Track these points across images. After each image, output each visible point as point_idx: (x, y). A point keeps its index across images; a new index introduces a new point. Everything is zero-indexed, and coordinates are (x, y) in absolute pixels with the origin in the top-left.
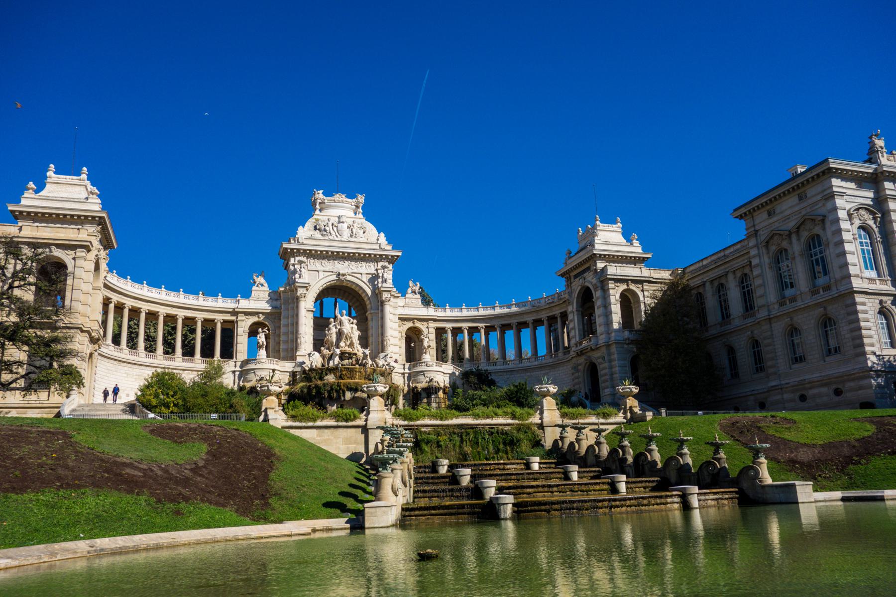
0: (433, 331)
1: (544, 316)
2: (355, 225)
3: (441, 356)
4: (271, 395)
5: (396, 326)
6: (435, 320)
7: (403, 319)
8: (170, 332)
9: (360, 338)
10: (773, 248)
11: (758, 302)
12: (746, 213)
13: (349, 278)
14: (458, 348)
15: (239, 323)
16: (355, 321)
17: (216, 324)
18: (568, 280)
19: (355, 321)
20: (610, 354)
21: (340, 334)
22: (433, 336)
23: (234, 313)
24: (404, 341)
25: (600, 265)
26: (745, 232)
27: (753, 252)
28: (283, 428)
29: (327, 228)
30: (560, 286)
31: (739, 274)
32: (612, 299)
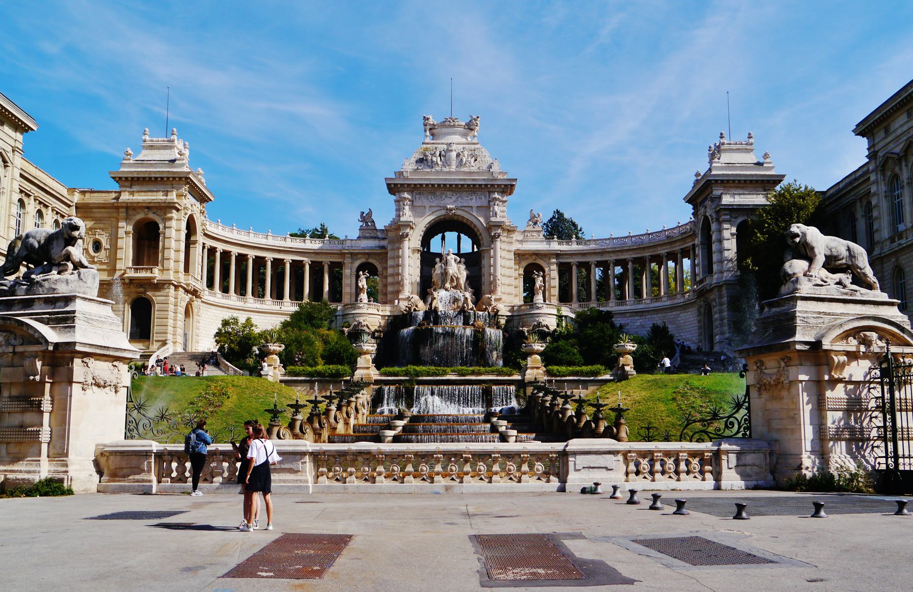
0: (554, 267)
1: (677, 248)
2: (466, 153)
3: (565, 297)
4: (272, 354)
5: (512, 263)
6: (558, 255)
7: (520, 256)
8: (259, 281)
9: (468, 277)
10: (889, 173)
11: (877, 237)
12: (865, 129)
13: (459, 212)
14: (585, 284)
16: (463, 260)
17: (323, 267)
18: (695, 208)
19: (463, 260)
20: (721, 297)
21: (445, 274)
22: (555, 274)
23: (342, 254)
24: (522, 280)
25: (717, 192)
26: (867, 153)
27: (873, 177)
28: (281, 381)
29: (434, 159)
30: (684, 215)
31: (864, 203)
32: (726, 234)
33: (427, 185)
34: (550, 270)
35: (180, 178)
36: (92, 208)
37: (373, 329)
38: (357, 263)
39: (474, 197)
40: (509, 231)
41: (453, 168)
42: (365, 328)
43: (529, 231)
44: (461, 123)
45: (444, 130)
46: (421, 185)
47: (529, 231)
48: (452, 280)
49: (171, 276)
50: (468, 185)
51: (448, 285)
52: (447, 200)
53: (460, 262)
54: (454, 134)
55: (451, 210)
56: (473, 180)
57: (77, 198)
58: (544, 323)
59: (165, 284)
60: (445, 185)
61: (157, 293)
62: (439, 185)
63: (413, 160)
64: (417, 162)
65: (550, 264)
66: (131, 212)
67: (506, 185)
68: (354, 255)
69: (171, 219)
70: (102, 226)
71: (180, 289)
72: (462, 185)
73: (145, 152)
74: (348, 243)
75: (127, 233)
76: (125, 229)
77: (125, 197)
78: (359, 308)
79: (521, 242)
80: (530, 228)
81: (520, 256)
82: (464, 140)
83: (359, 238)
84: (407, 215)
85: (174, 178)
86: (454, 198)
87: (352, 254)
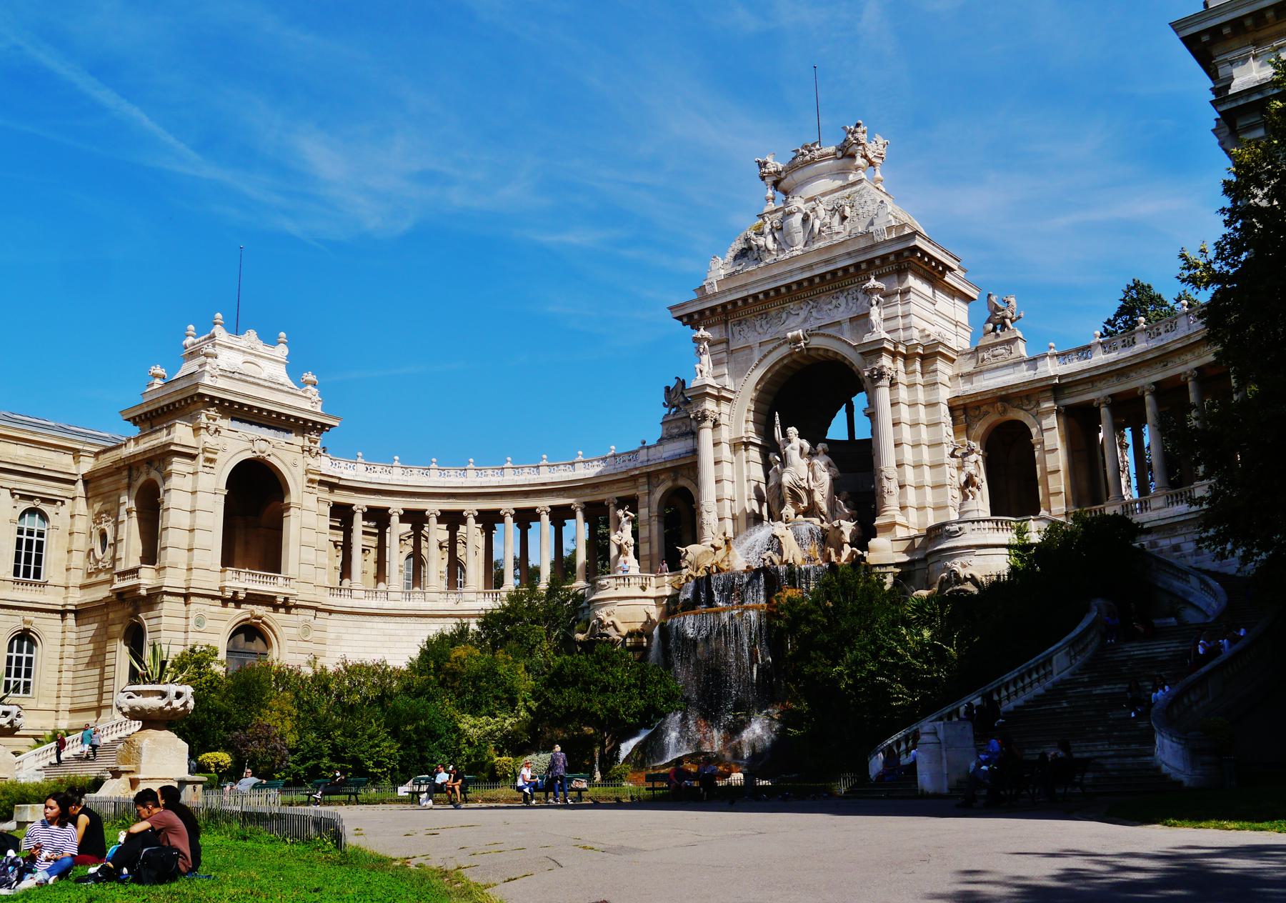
0: (1052, 421)
6: (1057, 388)
7: (963, 411)
9: (837, 487)
13: (816, 342)
15: (643, 500)
23: (634, 479)
33: (745, 299)
34: (1042, 431)
35: (192, 397)
36: (100, 478)
37: (624, 630)
38: (659, 493)
39: (842, 300)
40: (923, 358)
41: (799, 249)
42: (611, 631)
43: (987, 348)
44: (824, 150)
45: (799, 176)
46: (734, 303)
47: (987, 348)
48: (796, 498)
49: (174, 580)
50: (822, 276)
51: (789, 510)
52: (792, 321)
53: (812, 454)
54: (818, 176)
55: (796, 340)
56: (827, 262)
57: (87, 465)
58: (963, 573)
59: (157, 595)
60: (777, 290)
61: (151, 614)
62: (766, 293)
63: (730, 255)
64: (736, 258)
65: (1039, 416)
66: (134, 473)
67: (898, 254)
68: (651, 477)
69: (170, 475)
70: (108, 506)
71: (193, 599)
72: (811, 280)
73: (185, 366)
74: (643, 456)
75: (129, 512)
76: (128, 502)
77: (132, 449)
78: (602, 587)
79: (968, 376)
80: (991, 339)
81: (963, 411)
82: (839, 183)
83: (661, 441)
84: (705, 373)
85: (185, 399)
86: (803, 314)
87: (648, 475)
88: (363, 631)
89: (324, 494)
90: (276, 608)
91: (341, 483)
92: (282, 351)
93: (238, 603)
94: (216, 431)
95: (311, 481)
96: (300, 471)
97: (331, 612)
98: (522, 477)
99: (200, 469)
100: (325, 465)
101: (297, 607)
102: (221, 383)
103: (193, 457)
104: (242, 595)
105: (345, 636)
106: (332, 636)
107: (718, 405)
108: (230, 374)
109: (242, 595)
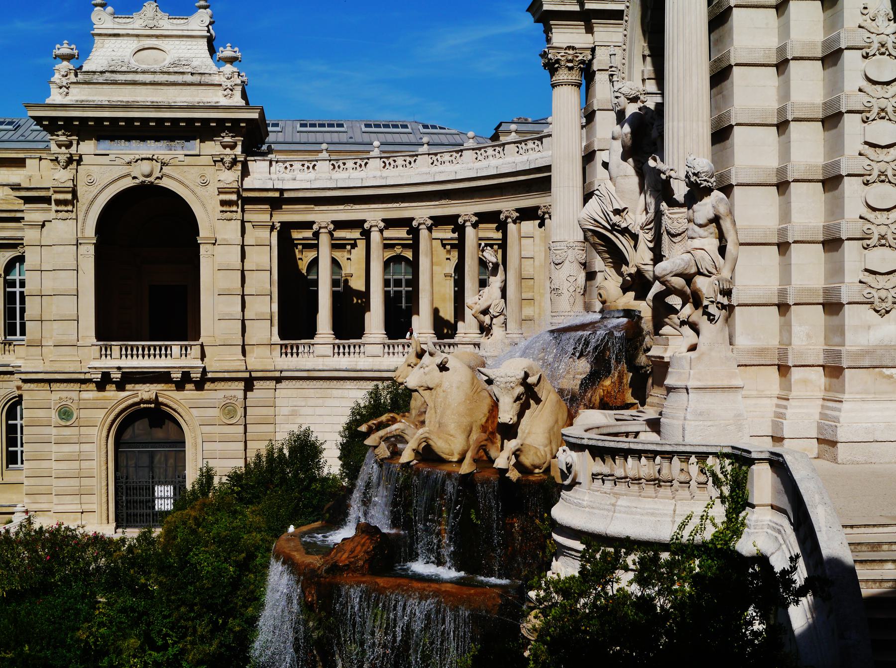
88: (329, 402)
89: (259, 215)
90: (180, 386)
91: (286, 195)
92: (199, 22)
93: (120, 387)
94: (70, 161)
95: (223, 203)
96: (212, 189)
97: (278, 380)
98: (509, 159)
99: (53, 215)
100: (263, 175)
101: (213, 380)
102: (78, 94)
103: (47, 200)
104: (116, 376)
105: (303, 411)
106: (286, 411)
107: (589, 30)
108: (111, 77)
109: (116, 376)
